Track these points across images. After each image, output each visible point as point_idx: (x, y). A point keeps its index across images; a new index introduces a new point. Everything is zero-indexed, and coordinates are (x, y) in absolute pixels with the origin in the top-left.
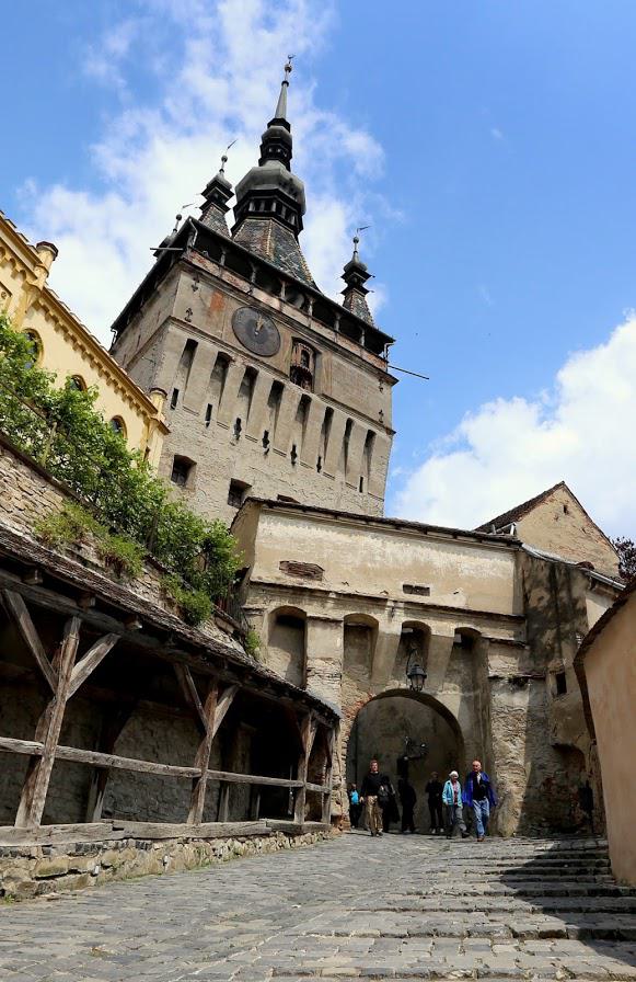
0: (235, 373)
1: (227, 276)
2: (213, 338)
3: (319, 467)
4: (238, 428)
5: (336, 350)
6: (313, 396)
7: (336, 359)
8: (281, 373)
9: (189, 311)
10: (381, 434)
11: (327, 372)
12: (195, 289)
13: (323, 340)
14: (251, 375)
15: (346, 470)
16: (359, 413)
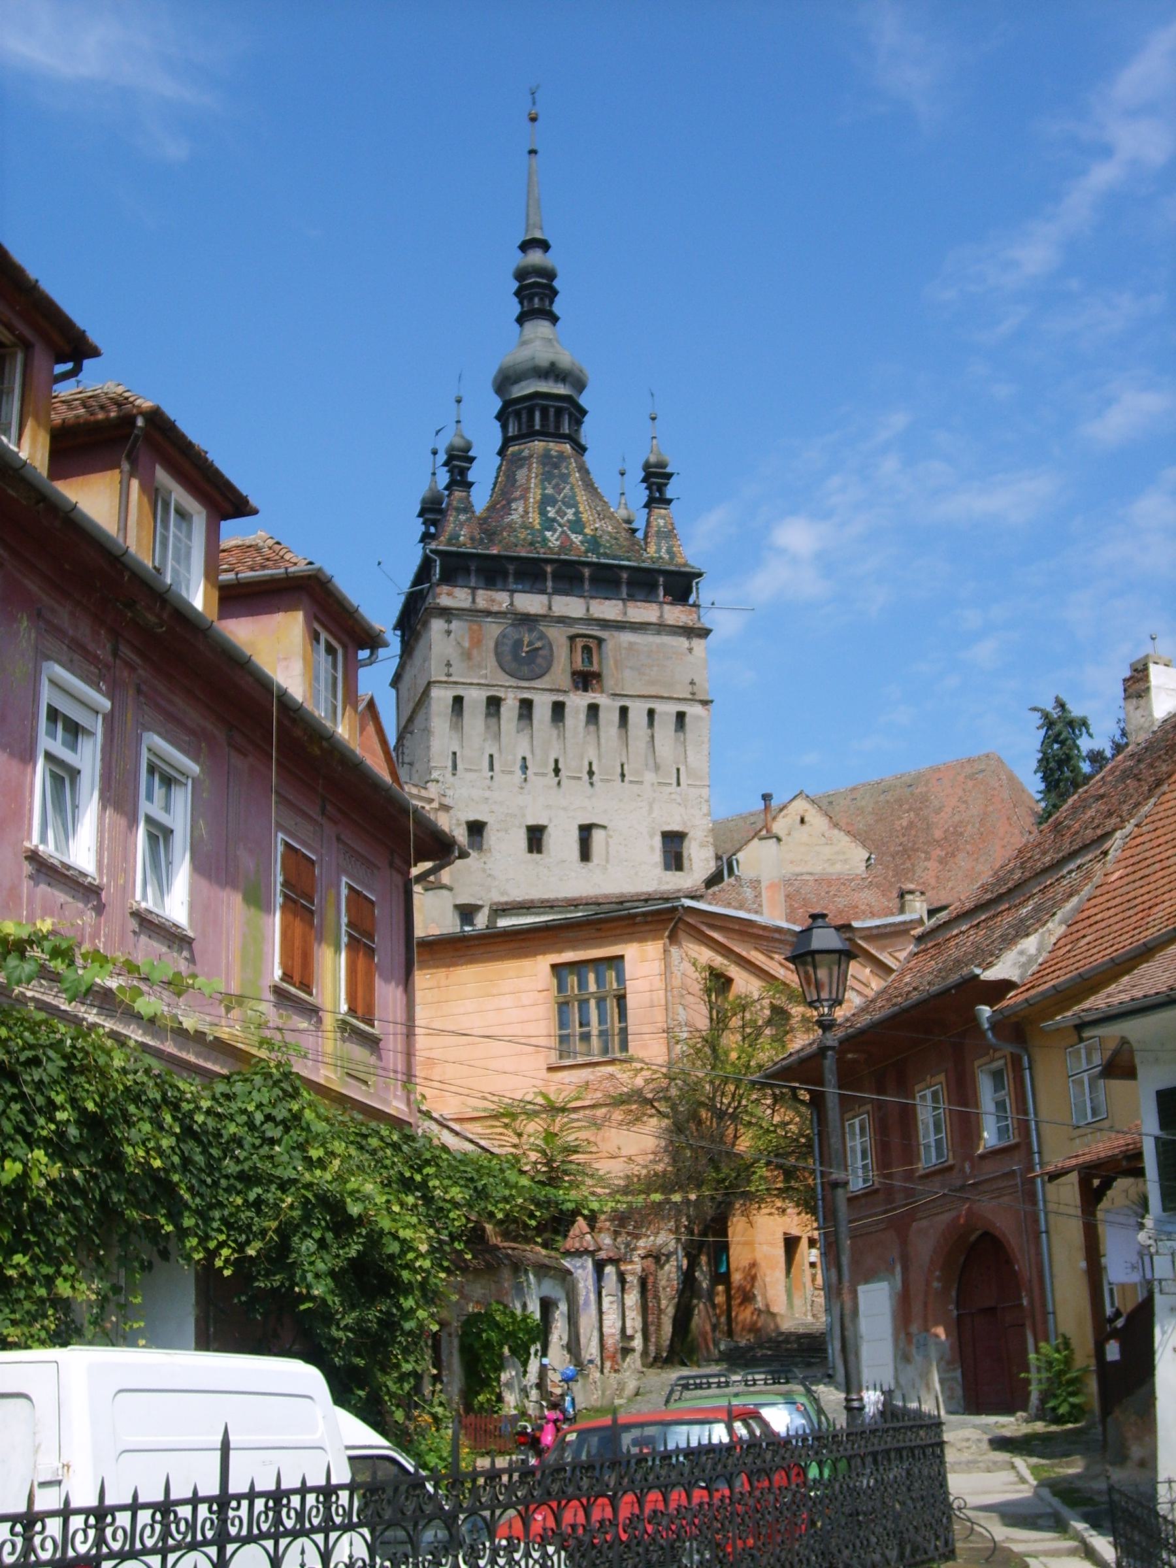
0: (510, 708)
1: (484, 598)
2: (478, 684)
3: (623, 775)
4: (525, 768)
5: (625, 628)
6: (601, 699)
7: (626, 637)
8: (558, 691)
9: (449, 665)
10: (693, 711)
11: (616, 662)
12: (449, 632)
13: (605, 624)
14: (526, 706)
15: (657, 768)
16: (662, 698)
